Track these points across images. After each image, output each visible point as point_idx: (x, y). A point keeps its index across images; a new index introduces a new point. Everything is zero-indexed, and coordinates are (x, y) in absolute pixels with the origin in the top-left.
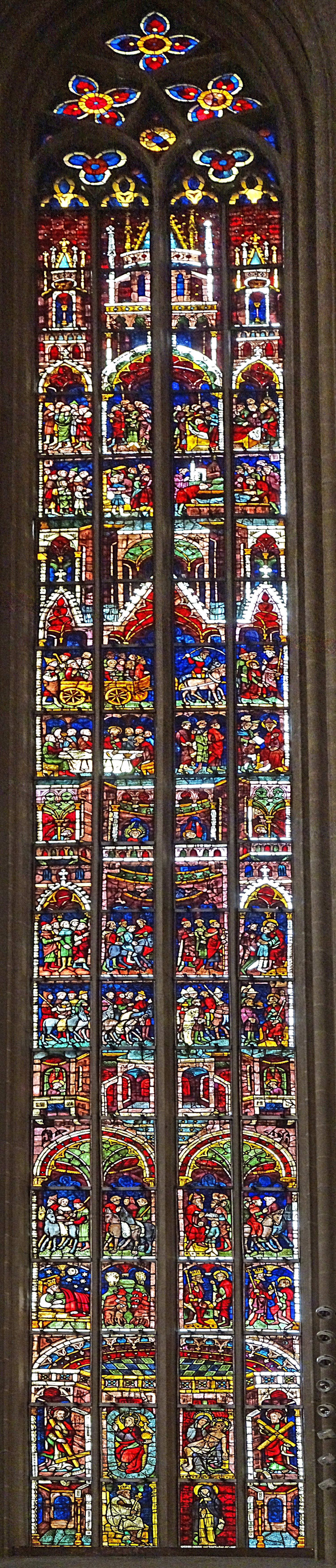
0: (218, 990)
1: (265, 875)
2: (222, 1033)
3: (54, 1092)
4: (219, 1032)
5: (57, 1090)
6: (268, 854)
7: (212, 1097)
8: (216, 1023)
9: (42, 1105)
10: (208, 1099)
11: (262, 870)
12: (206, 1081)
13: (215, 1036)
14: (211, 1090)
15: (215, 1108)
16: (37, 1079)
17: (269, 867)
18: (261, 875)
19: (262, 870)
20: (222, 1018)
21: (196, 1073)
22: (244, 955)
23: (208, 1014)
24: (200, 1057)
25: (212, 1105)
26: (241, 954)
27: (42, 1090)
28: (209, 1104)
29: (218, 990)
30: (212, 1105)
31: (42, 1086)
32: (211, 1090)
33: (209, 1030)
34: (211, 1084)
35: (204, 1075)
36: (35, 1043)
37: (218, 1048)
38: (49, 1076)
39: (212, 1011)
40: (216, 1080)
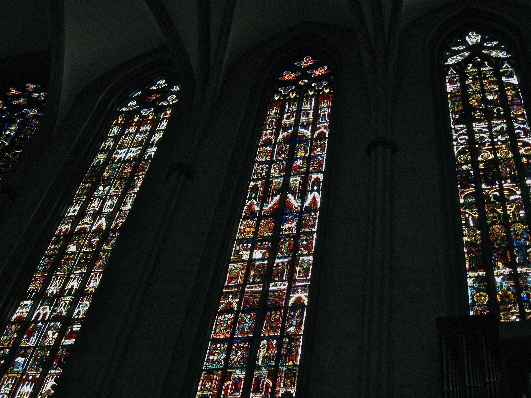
0: (275, 341)
1: (300, 292)
2: (273, 359)
3: (205, 389)
4: (272, 359)
5: (207, 388)
6: (302, 284)
7: (264, 390)
8: (272, 355)
9: (200, 395)
10: (262, 390)
11: (299, 290)
12: (263, 381)
13: (270, 361)
14: (264, 385)
15: (264, 394)
16: (200, 383)
17: (301, 289)
18: (298, 292)
19: (299, 290)
20: (274, 352)
21: (260, 378)
22: (287, 325)
23: (269, 351)
24: (263, 371)
25: (263, 393)
26: (286, 325)
27: (201, 388)
28: (262, 392)
29: (275, 341)
30: (263, 393)
31: (202, 386)
32: (264, 385)
33: (269, 358)
34: (265, 383)
35: (263, 379)
36: (204, 366)
37: (270, 366)
38: (205, 381)
39: (271, 350)
40: (267, 381)
